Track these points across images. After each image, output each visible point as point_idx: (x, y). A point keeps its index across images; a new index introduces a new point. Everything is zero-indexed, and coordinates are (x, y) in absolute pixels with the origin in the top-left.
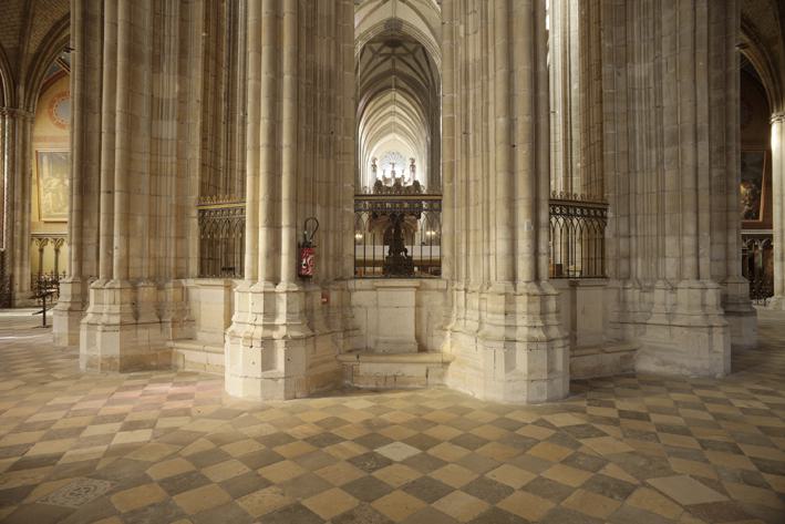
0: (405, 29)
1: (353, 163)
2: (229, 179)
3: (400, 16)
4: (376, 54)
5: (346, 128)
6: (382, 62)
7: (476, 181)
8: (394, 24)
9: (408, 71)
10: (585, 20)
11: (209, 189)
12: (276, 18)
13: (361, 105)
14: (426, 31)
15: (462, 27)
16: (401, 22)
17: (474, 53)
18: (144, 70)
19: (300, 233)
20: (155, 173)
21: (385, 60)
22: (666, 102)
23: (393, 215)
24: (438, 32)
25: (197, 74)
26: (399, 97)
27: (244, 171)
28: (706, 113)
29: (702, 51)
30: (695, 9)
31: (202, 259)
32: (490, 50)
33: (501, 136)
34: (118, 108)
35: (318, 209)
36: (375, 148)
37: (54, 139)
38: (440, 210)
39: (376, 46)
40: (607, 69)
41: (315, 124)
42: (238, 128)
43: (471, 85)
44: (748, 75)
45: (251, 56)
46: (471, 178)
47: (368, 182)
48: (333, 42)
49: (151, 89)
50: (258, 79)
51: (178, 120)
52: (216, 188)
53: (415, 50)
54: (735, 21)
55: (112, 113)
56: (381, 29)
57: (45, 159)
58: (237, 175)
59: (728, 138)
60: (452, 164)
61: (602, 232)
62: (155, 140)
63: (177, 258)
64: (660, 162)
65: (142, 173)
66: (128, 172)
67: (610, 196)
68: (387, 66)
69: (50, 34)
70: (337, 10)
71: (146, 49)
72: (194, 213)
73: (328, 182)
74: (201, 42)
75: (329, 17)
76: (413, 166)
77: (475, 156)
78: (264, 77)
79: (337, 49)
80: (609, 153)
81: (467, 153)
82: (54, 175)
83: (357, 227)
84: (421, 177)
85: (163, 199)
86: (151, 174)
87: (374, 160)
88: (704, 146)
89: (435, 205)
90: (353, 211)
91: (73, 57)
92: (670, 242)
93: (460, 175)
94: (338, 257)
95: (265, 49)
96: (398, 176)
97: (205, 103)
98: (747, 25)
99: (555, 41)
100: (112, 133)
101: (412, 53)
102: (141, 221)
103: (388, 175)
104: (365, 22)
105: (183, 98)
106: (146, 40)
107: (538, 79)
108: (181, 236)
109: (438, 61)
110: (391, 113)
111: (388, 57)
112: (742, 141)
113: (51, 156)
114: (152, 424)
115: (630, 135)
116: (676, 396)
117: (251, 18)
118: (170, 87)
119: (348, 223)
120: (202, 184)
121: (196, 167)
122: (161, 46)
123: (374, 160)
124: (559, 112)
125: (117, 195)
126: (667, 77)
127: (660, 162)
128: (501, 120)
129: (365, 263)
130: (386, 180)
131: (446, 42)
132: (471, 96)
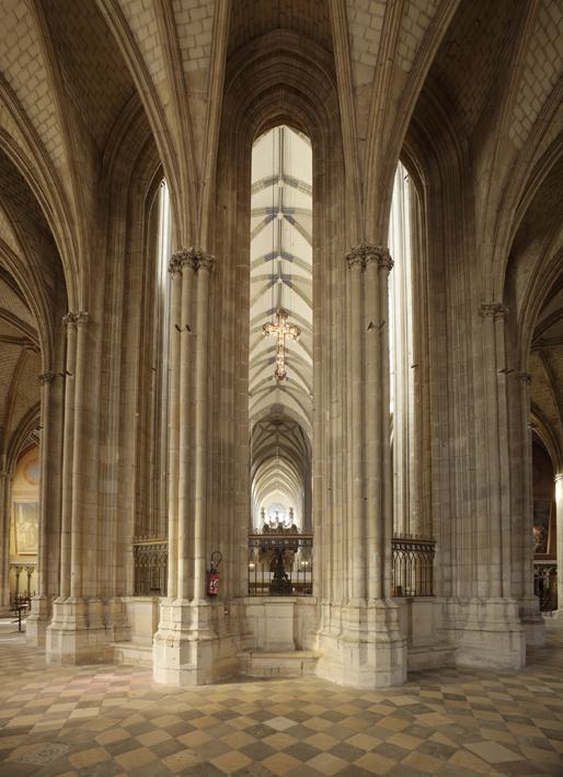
0: (286, 411)
1: (247, 511)
2: (157, 522)
4: (264, 430)
5: (243, 486)
7: (338, 525)
8: (278, 408)
10: (419, 406)
11: (141, 531)
12: (190, 404)
13: (253, 468)
14: (302, 414)
15: (328, 413)
17: (337, 431)
19: (209, 562)
20: (102, 519)
22: (478, 466)
23: (277, 550)
24: (311, 415)
25: (132, 443)
26: (281, 463)
27: (167, 517)
28: (507, 474)
29: (504, 429)
30: (497, 399)
31: (136, 582)
32: (349, 430)
33: (356, 492)
34: (74, 471)
35: (222, 545)
37: (26, 493)
38: (311, 546)
39: (264, 425)
41: (219, 483)
42: (162, 485)
43: (334, 456)
44: (537, 446)
45: (172, 432)
46: (335, 522)
47: (258, 526)
48: (232, 424)
49: (99, 456)
50: (177, 448)
51: (119, 480)
52: (147, 530)
53: (294, 427)
55: (70, 474)
56: (268, 411)
57: (21, 509)
58: (162, 520)
59: (523, 492)
60: (320, 512)
61: (431, 562)
62: (102, 495)
63: (117, 581)
64: (474, 511)
65: (91, 519)
66: (82, 518)
67: (437, 536)
68: (273, 439)
71: (95, 427)
72: (131, 548)
73: (229, 525)
74: (135, 420)
75: (230, 403)
76: (291, 514)
77: (337, 505)
78: (181, 448)
79: (236, 427)
80: (436, 504)
81: (331, 503)
82: (26, 520)
83: (250, 559)
84: (298, 521)
85: (108, 538)
86: (98, 520)
87: (263, 509)
88: (506, 499)
89: (308, 543)
90: (247, 546)
91: (42, 434)
92: (481, 570)
93: (326, 521)
94: (236, 581)
95: (182, 428)
96: (281, 521)
97: (138, 466)
98: (535, 409)
99: (398, 422)
100: (70, 488)
101: (292, 430)
102: (91, 554)
103: (273, 520)
104: (256, 406)
105: (122, 463)
106: (95, 420)
107: (385, 453)
108: (120, 565)
109: (310, 436)
111: (273, 433)
112: (535, 495)
113: (26, 506)
115: (451, 491)
118: (112, 455)
119: (244, 556)
120: (136, 527)
121: (132, 513)
123: (263, 509)
124: (400, 473)
125: (73, 535)
126: (478, 448)
127: (474, 511)
128: (357, 480)
129: (256, 585)
130: (272, 524)
131: (316, 424)
132: (334, 464)
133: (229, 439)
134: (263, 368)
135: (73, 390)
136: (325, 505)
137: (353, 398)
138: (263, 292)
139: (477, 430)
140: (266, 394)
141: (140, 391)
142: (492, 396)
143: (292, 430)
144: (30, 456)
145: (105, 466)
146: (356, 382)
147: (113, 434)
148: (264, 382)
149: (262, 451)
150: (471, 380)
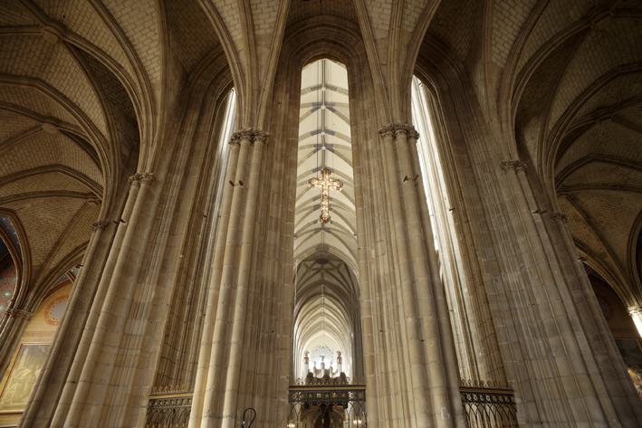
0: (331, 251)
1: (289, 357)
2: (182, 370)
3: (327, 242)
4: (309, 269)
5: (284, 327)
6: (314, 275)
7: (393, 372)
8: (323, 248)
9: (335, 282)
10: (463, 244)
11: (162, 380)
13: (296, 307)
14: (347, 252)
15: (373, 251)
16: (328, 246)
17: (384, 268)
18: (131, 281)
19: (239, 423)
20: (119, 365)
21: (317, 273)
23: (323, 406)
24: (356, 253)
25: (170, 284)
26: (327, 301)
27: (195, 363)
28: (572, 308)
29: (554, 263)
30: (539, 235)
32: (396, 266)
33: (411, 332)
34: (103, 309)
35: (257, 399)
36: (307, 344)
37: (40, 334)
38: (365, 400)
40: (486, 277)
41: (259, 324)
43: (383, 293)
44: (595, 279)
45: (214, 272)
46: (390, 369)
47: (301, 375)
48: (277, 263)
49: (133, 295)
50: (218, 289)
51: (149, 319)
52: (169, 378)
53: (339, 265)
54: (570, 243)
55: (97, 314)
56: (314, 251)
57: (26, 353)
58: (189, 367)
59: (599, 329)
61: (515, 418)
62: (126, 336)
67: (513, 382)
68: (318, 277)
69: (68, 256)
70: (281, 240)
71: (137, 266)
72: (145, 403)
73: (267, 374)
74: (178, 261)
75: (275, 246)
76: (339, 358)
77: (391, 350)
78: (222, 287)
80: (503, 343)
81: (384, 347)
82: (27, 366)
83: (290, 418)
84: (347, 368)
85: (121, 388)
86: (115, 366)
87: (307, 353)
88: (580, 335)
89: (360, 392)
90: (287, 401)
91: (80, 273)
93: (380, 368)
95: (225, 268)
96: (327, 367)
97: (172, 307)
98: (580, 244)
99: (444, 258)
100: (92, 329)
101: (337, 268)
103: (319, 367)
104: (301, 247)
105: (156, 302)
106: (138, 260)
107: (436, 289)
109: (356, 273)
110: (320, 314)
111: (318, 271)
112: (613, 331)
113: (33, 349)
117: (218, 246)
118: (148, 293)
119: (282, 414)
120: (158, 374)
121: (156, 358)
122: (149, 263)
123: (307, 353)
124: (456, 310)
125: (80, 384)
126: (533, 283)
127: (549, 350)
128: (410, 320)
130: (317, 371)
131: (362, 261)
132: (384, 301)
133: (273, 278)
134: (307, 214)
135: (123, 236)
136: (378, 350)
137: (397, 236)
138: (309, 156)
139: (527, 265)
140: (311, 236)
141: (187, 237)
142: (532, 233)
143: (337, 268)
144: (61, 292)
145: (138, 305)
146: (398, 224)
147: (154, 272)
148: (309, 225)
149: (308, 289)
150: (508, 220)
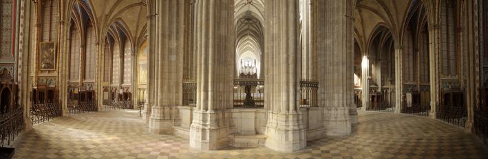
3: (251, 10)
9: (254, 29)
11: (185, 77)
12: (207, 20)
17: (275, 30)
18: (167, 40)
20: (170, 72)
22: (335, 53)
25: (182, 39)
31: (183, 99)
40: (319, 39)
44: (356, 44)
50: (201, 41)
55: (158, 54)
60: (268, 69)
62: (170, 62)
63: (176, 99)
64: (333, 71)
66: (162, 72)
67: (319, 80)
70: (228, 15)
71: (167, 33)
79: (228, 28)
80: (319, 66)
89: (262, 82)
92: (336, 95)
93: (270, 73)
94: (228, 101)
97: (184, 48)
100: (158, 61)
102: (166, 87)
105: (177, 48)
108: (177, 92)
114: (168, 155)
115: (325, 61)
116: (338, 143)
117: (199, 20)
118: (174, 44)
121: (182, 69)
122: (171, 32)
125: (159, 80)
128: (285, 56)
129: (237, 101)
135: (158, 21)
136: (270, 66)
137: (283, 16)
139: (335, 37)
141: (185, 16)
144: (144, 45)
145: (171, 49)
146: (284, 9)
147: (174, 35)
